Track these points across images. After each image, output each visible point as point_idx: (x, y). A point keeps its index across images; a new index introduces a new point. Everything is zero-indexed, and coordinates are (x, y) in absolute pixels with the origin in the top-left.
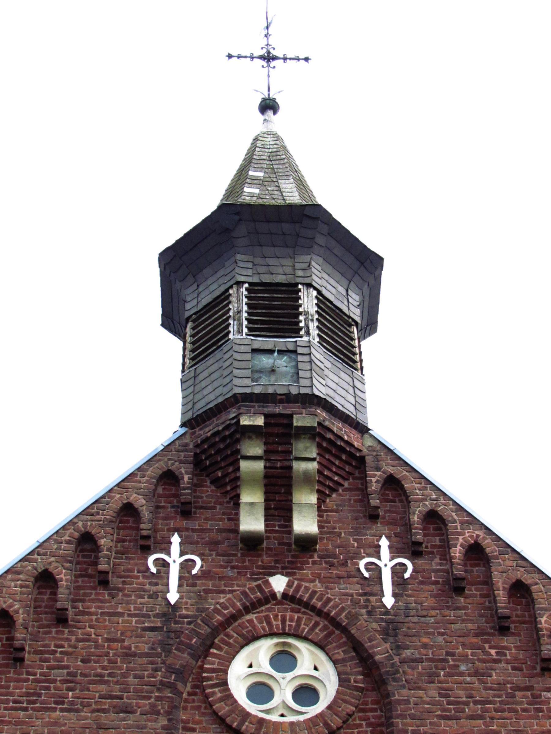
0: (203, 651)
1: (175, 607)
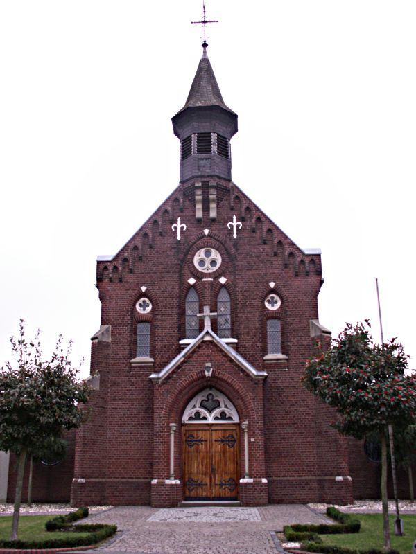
0: (186, 254)
1: (180, 241)
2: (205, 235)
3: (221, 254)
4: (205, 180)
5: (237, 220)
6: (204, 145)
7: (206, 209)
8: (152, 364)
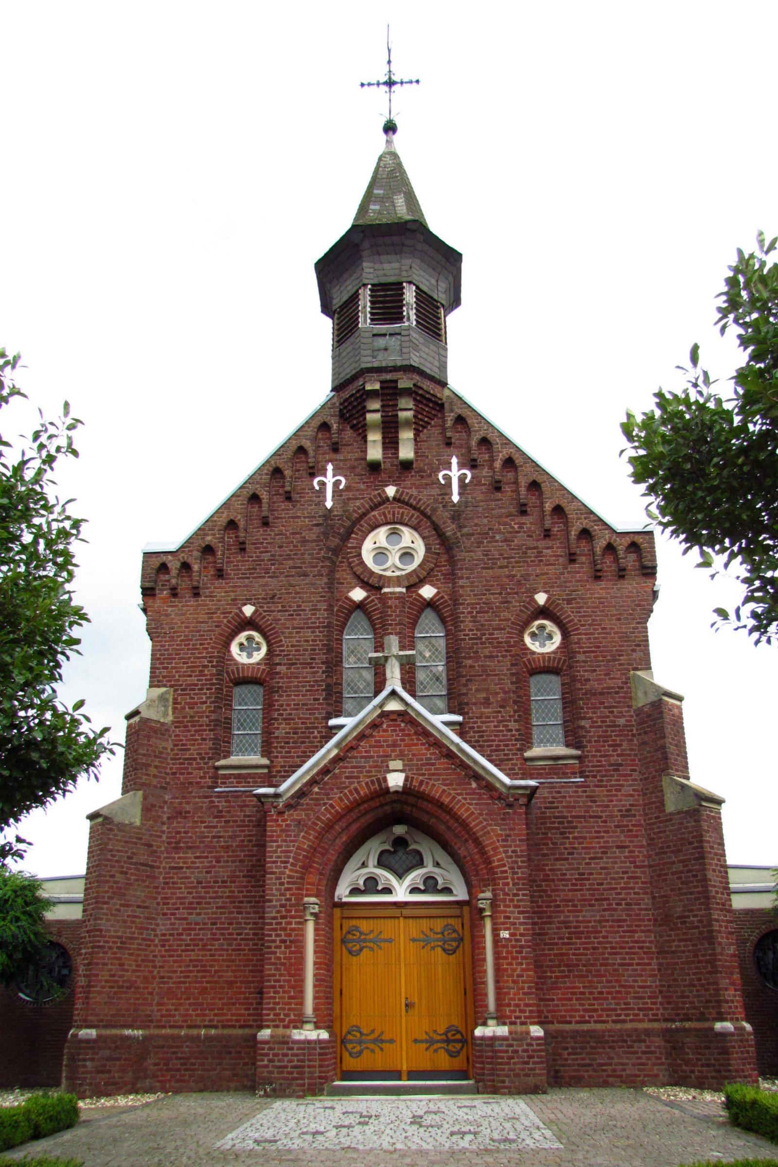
0: (346, 538)
1: (330, 511)
2: (388, 499)
3: (423, 538)
4: (389, 377)
5: (461, 466)
6: (388, 306)
7: (391, 443)
8: (266, 771)
